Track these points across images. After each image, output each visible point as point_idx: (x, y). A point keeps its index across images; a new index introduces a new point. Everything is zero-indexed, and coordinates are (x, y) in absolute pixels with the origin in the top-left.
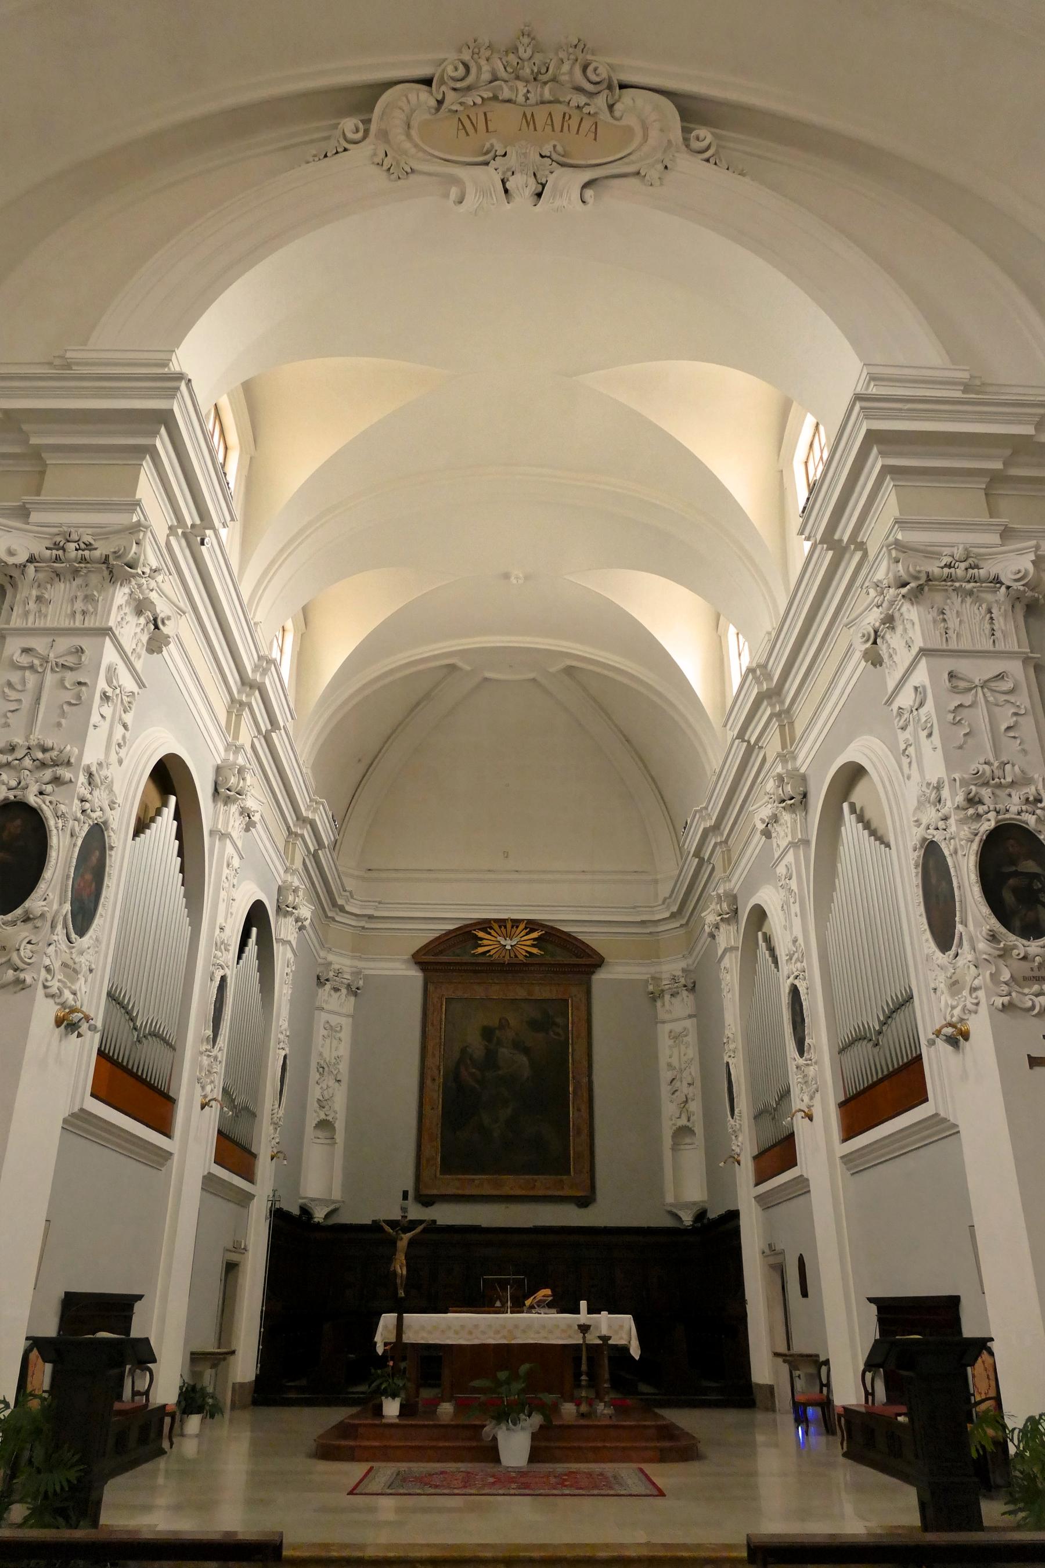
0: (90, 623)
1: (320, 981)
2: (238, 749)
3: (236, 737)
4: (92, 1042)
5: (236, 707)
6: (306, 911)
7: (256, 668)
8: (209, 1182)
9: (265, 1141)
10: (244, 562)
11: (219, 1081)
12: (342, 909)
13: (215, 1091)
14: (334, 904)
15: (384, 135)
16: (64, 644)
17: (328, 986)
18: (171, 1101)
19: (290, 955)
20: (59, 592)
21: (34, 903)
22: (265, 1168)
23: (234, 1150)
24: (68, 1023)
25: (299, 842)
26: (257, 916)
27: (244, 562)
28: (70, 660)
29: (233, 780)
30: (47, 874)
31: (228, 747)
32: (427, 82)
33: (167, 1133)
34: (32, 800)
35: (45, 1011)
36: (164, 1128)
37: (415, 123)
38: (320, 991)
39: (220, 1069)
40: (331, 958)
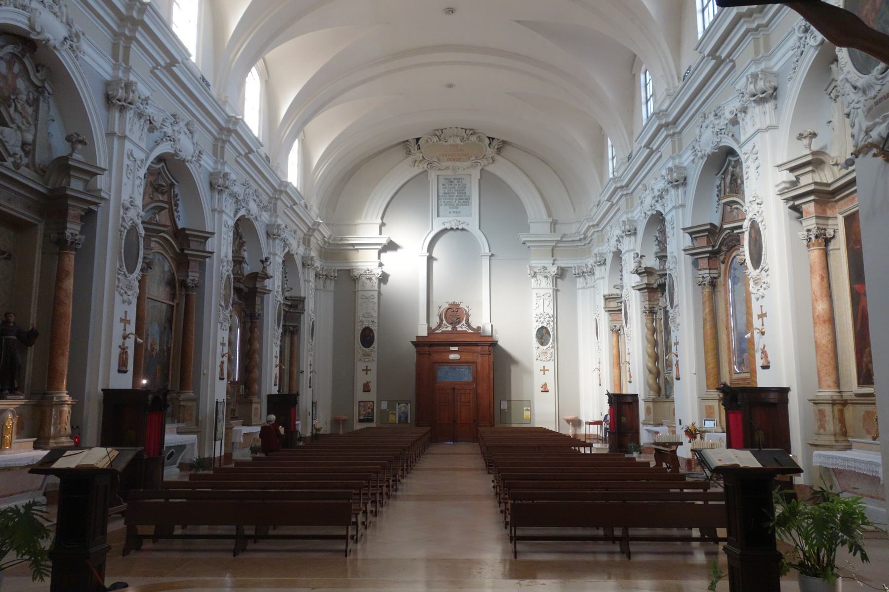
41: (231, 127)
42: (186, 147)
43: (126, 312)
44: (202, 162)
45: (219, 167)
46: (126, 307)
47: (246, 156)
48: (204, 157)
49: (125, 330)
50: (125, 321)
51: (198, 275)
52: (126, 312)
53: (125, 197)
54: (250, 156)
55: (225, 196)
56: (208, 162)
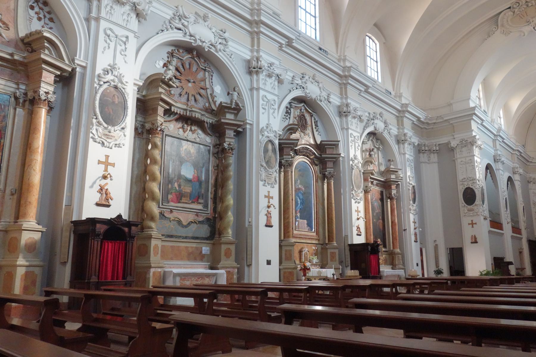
0: (471, 154)
1: (529, 182)
2: (497, 150)
3: (496, 148)
4: (489, 219)
5: (494, 141)
6: (521, 171)
7: (497, 132)
8: (512, 237)
9: (522, 226)
10: (488, 110)
11: (509, 218)
12: (531, 162)
13: (509, 220)
14: (528, 161)
15: (502, 26)
16: (468, 159)
17: (532, 183)
18: (502, 224)
19: (519, 183)
20: (464, 149)
21: (476, 203)
22: (524, 232)
23: (516, 230)
24: (485, 219)
25: (515, 155)
26: (510, 179)
27: (488, 110)
28: (470, 162)
29: (498, 158)
30: (477, 198)
31: (495, 150)
32: (510, 8)
33: (502, 230)
34: (471, 187)
35: (482, 218)
36: (501, 229)
37: (509, 20)
38: (529, 184)
39: (509, 215)
40: (531, 175)
41: (346, 73)
42: (313, 91)
43: (269, 192)
44: (331, 100)
45: (344, 101)
46: (269, 188)
47: (366, 91)
48: (332, 96)
49: (269, 202)
50: (269, 197)
51: (333, 170)
52: (269, 192)
53: (263, 124)
54: (369, 90)
55: (350, 118)
56: (336, 100)
